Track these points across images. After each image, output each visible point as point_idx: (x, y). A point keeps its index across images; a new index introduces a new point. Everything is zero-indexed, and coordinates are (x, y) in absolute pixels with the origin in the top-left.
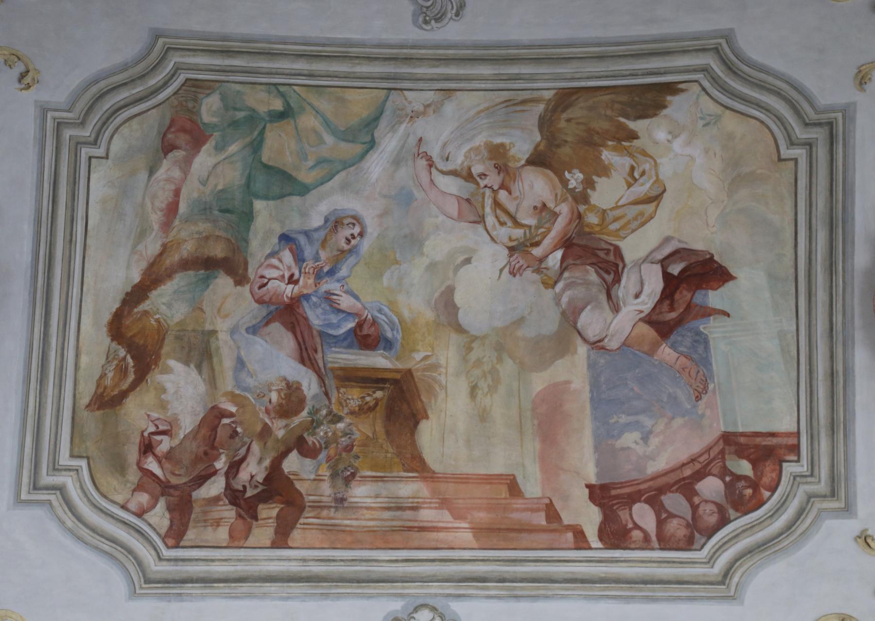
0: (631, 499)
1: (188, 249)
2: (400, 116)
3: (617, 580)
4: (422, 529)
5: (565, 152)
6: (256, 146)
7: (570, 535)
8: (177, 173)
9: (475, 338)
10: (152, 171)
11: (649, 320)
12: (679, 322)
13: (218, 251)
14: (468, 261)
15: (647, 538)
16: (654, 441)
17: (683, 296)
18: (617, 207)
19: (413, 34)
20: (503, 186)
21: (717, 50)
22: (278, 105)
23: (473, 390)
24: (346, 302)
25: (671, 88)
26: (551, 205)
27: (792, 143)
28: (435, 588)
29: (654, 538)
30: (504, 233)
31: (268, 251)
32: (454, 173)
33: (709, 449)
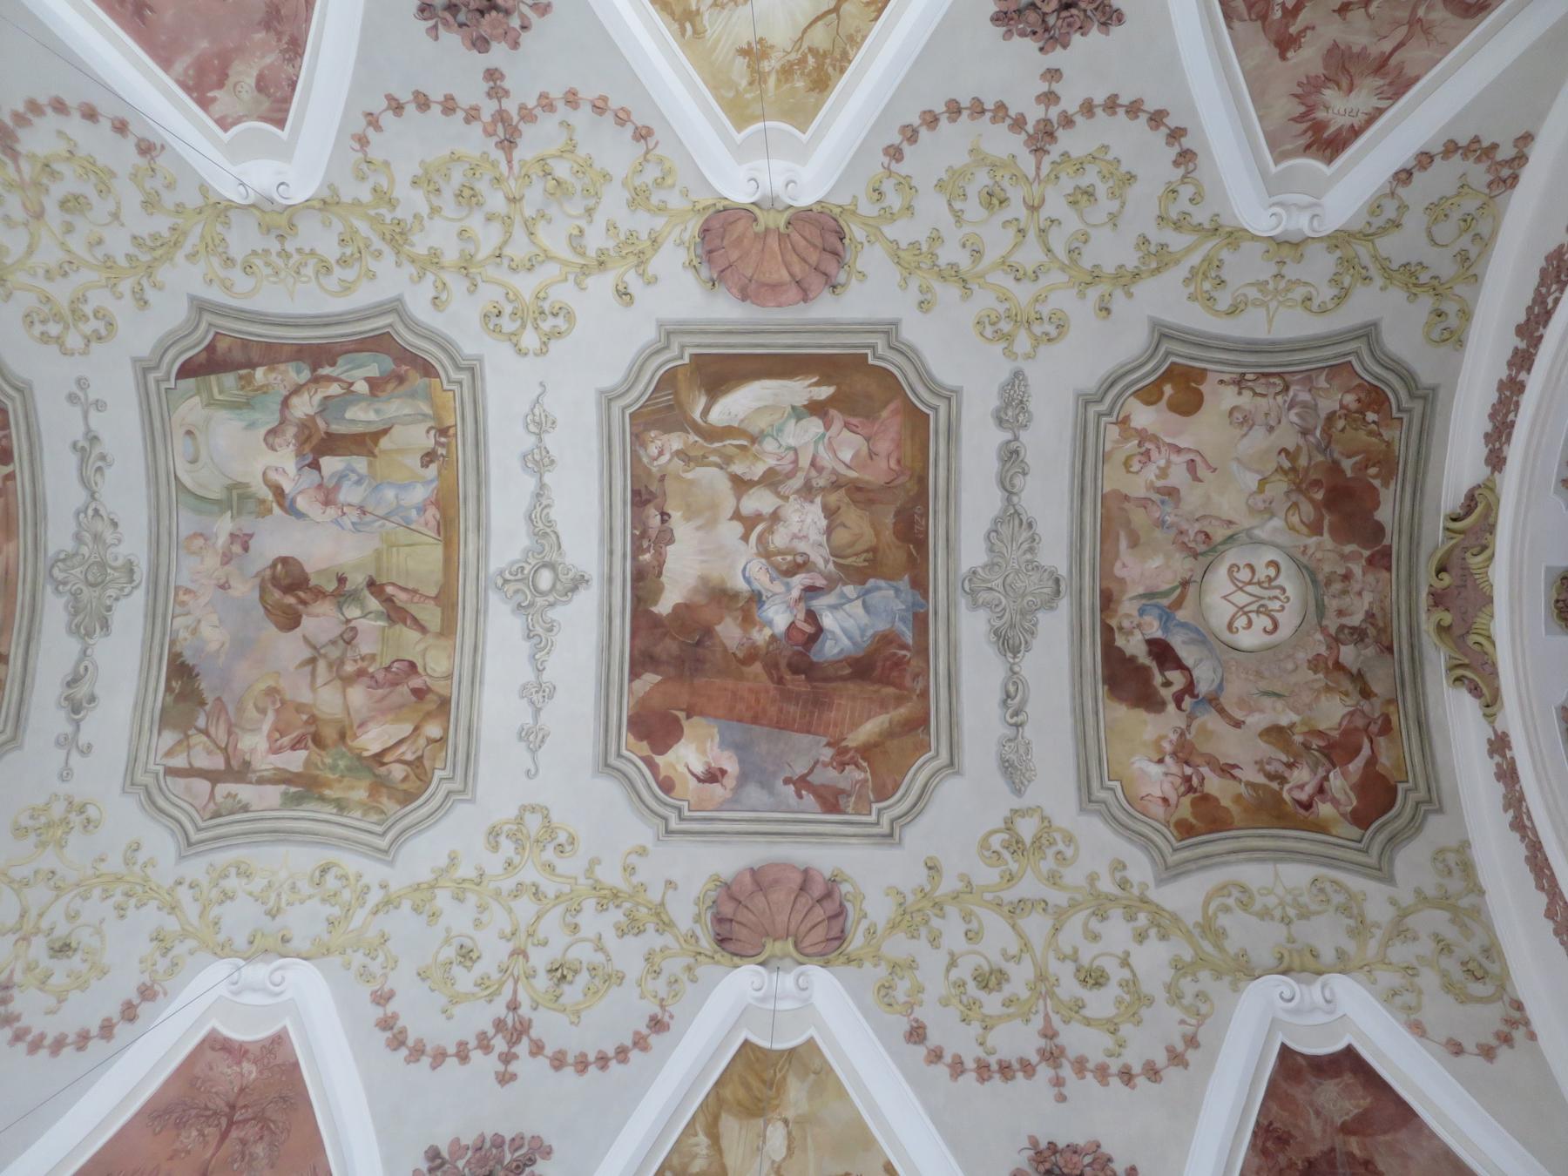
3: (31, 453)
4: (7, 573)
7: (9, 483)
28: (41, 565)
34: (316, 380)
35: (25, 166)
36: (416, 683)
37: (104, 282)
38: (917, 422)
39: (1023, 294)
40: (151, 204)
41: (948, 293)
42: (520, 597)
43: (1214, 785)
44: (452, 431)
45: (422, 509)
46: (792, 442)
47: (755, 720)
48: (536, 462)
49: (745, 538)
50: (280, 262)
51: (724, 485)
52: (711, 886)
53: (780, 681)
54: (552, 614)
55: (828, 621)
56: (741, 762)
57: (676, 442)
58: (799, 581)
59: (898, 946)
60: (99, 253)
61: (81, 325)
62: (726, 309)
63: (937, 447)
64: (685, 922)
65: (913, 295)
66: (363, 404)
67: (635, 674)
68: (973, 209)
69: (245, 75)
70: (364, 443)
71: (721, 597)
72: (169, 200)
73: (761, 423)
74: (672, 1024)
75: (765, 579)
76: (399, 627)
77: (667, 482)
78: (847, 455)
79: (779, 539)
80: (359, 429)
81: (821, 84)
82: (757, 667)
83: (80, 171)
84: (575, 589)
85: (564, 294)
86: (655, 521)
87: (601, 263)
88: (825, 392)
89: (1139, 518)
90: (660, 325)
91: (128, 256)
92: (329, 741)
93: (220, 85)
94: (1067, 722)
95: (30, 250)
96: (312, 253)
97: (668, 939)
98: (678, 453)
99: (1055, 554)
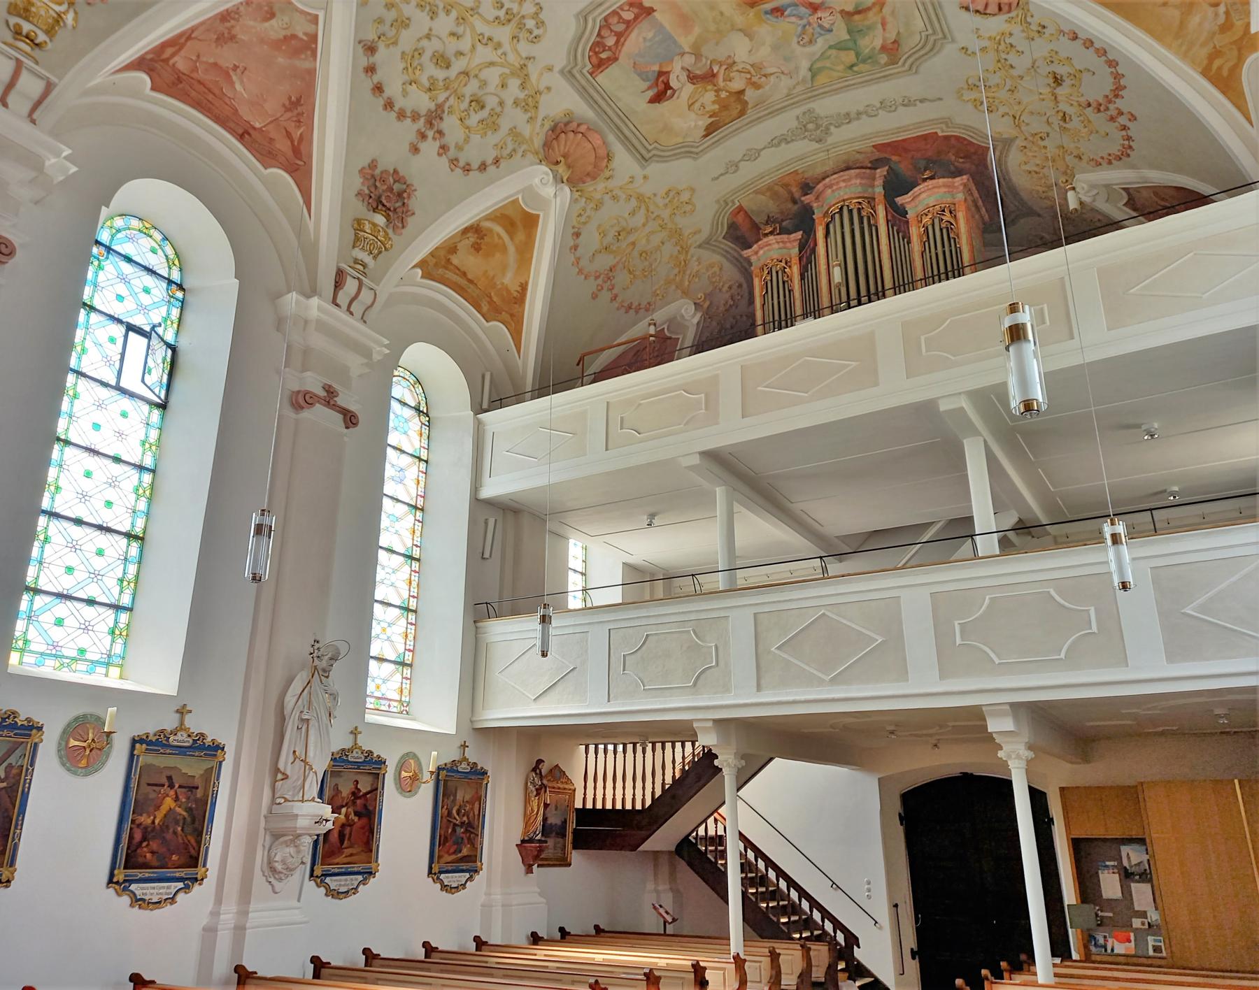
0: (636, 18)
1: (871, 14)
2: (804, 81)
5: (732, 99)
6: (857, 55)
8: (888, 35)
9: (732, 30)
10: (899, 33)
11: (668, 73)
12: (657, 79)
13: (857, 17)
14: (750, 52)
15: (622, 10)
16: (641, 39)
17: (661, 87)
18: (703, 95)
19: (812, 105)
20: (750, 79)
21: (697, 153)
22: (855, 69)
23: (722, 14)
24: (793, 19)
25: (706, 136)
26: (728, 83)
27: (655, 148)
29: (620, 11)
30: (740, 67)
31: (836, 25)
32: (772, 74)
33: (620, 51)
35: (441, 99)
37: (476, 16)
40: (404, 23)
60: (460, 30)
61: (515, 11)
69: (275, 28)
72: (392, 15)
83: (417, 72)
91: (448, 12)
93: (294, 37)
95: (492, 64)
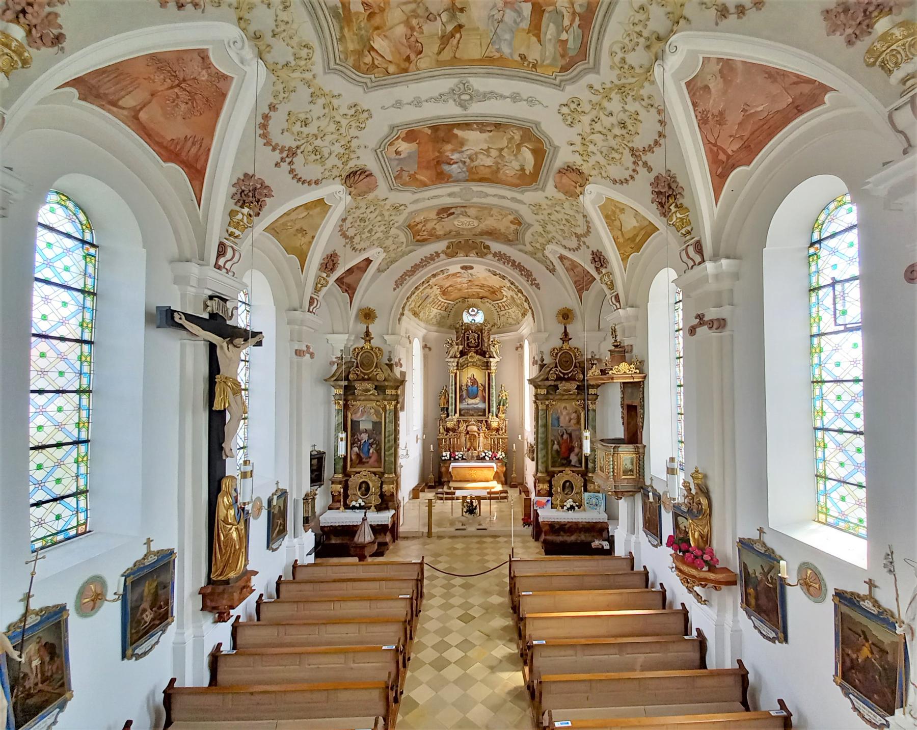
34: (574, 13)
36: (413, 56)
38: (517, 186)
39: (545, 213)
41: (549, 203)
42: (457, 89)
43: (420, 226)
44: (534, 70)
45: (498, 50)
46: (513, 162)
47: (419, 157)
48: (515, 97)
49: (481, 149)
50: (638, 29)
51: (501, 146)
52: (363, 167)
53: (433, 160)
54: (451, 101)
55: (454, 166)
56: (405, 158)
57: (517, 137)
58: (467, 160)
59: (363, 205)
62: (559, 163)
63: (508, 187)
64: (348, 167)
65: (550, 197)
66: (555, 34)
67: (429, 128)
68: (567, 217)
70: (536, 29)
71: (462, 144)
73: (519, 157)
74: (320, 185)
75: (469, 153)
76: (439, 42)
77: (503, 133)
78: (507, 172)
79: (481, 156)
80: (543, 29)
81: (607, 217)
82: (437, 154)
84: (461, 106)
85: (578, 128)
86: (489, 129)
87: (584, 145)
88: (527, 172)
89: (486, 212)
90: (558, 147)
92: (373, 22)
94: (431, 205)
96: (634, 49)
97: (341, 166)
98: (513, 138)
99: (475, 200)
